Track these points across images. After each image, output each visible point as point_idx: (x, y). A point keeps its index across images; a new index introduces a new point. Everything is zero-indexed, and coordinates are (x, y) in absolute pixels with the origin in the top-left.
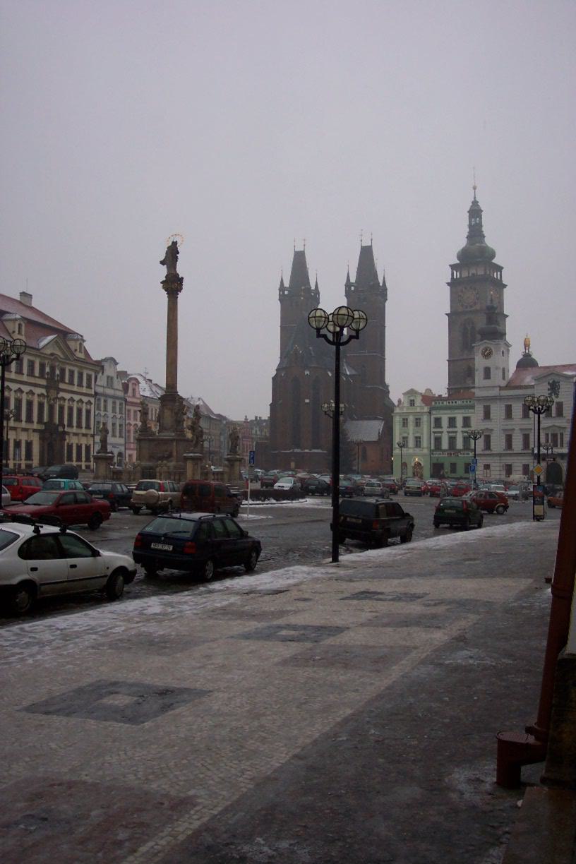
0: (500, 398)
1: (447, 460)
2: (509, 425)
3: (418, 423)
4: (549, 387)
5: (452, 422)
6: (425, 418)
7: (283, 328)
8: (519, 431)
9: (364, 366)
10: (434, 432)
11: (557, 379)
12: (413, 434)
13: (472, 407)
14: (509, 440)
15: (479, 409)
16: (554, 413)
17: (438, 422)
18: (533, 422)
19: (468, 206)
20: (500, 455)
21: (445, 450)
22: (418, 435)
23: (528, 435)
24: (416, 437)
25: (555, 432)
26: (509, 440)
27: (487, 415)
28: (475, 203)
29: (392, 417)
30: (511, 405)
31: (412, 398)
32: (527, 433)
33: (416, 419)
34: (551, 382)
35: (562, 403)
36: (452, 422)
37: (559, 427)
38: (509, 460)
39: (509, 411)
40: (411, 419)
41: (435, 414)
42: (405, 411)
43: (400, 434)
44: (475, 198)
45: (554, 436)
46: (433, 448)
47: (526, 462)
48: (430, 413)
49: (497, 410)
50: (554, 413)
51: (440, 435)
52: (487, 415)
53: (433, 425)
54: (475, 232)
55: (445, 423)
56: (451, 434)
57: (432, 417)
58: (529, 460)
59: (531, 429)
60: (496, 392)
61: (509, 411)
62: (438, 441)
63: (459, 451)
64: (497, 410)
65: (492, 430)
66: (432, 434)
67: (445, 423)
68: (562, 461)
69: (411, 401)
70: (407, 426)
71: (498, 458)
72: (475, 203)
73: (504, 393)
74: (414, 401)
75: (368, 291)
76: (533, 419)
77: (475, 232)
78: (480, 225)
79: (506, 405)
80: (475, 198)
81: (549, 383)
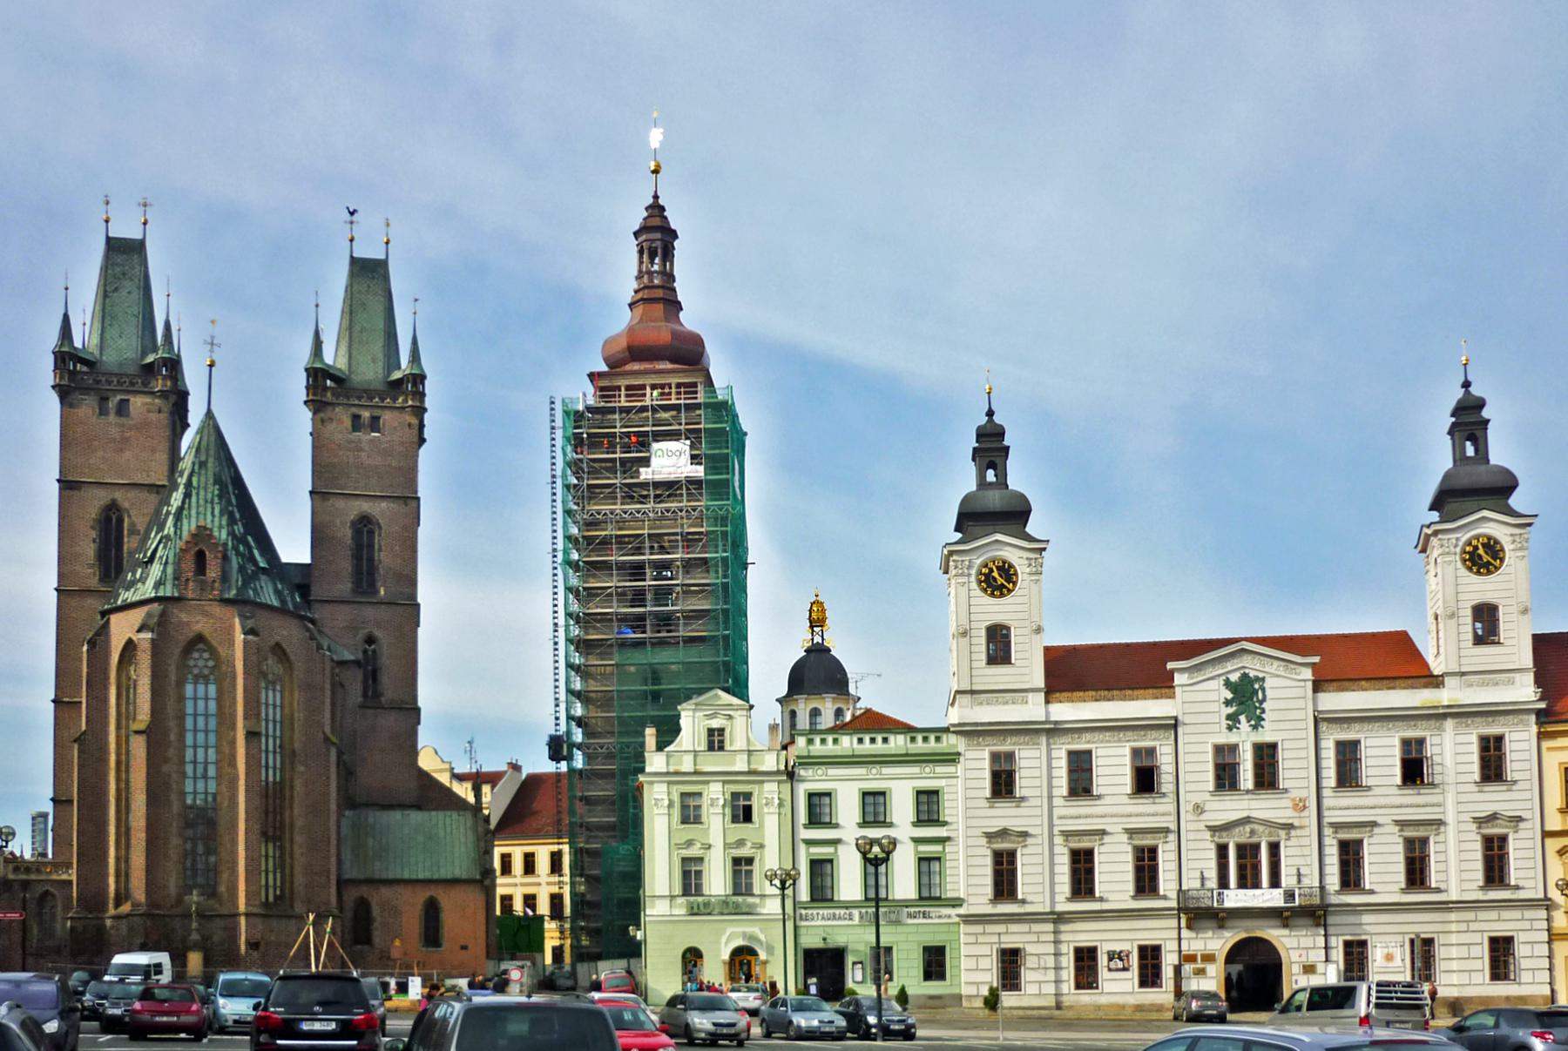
0: (1054, 730)
1: (853, 935)
2: (1080, 815)
3: (743, 813)
4: (1230, 696)
5: (874, 806)
6: (767, 796)
7: (67, 485)
8: (1125, 838)
9: (370, 640)
10: (810, 843)
11: (1253, 666)
12: (726, 846)
13: (951, 758)
14: (1082, 864)
15: (977, 764)
16: (1247, 776)
17: (819, 809)
18: (1172, 808)
19: (638, 217)
20: (1059, 918)
21: (848, 905)
22: (744, 852)
23: (1153, 851)
24: (737, 861)
25: (1254, 840)
26: (1082, 864)
27: (1003, 784)
28: (656, 209)
29: (640, 788)
30: (1089, 752)
31: (715, 724)
32: (1084, 844)
33: (735, 796)
34: (1234, 677)
35: (1274, 746)
36: (874, 806)
37: (1266, 823)
38: (1081, 935)
39: (1080, 766)
40: (715, 795)
41: (814, 780)
42: (687, 765)
43: (672, 846)
44: (656, 197)
45: (1248, 852)
46: (804, 894)
47: (1149, 938)
48: (791, 775)
49: (1040, 768)
50: (1247, 776)
51: (830, 850)
52: (1003, 784)
53: (802, 816)
54: (659, 294)
55: (847, 809)
56: (922, 848)
57: (802, 790)
58: (1162, 933)
59: (1167, 831)
60: (1034, 709)
61: (1080, 766)
62: (821, 869)
63: (906, 904)
64: (1040, 768)
65: (1025, 835)
66: (802, 848)
67: (847, 809)
68: (1286, 932)
69: (711, 732)
70: (697, 820)
71: (1050, 927)
72: (656, 209)
73: (1067, 711)
74: (721, 731)
75: (367, 404)
76: (1172, 797)
77: (659, 294)
78: (671, 277)
79: (1071, 753)
80: (656, 197)
81: (1228, 684)
